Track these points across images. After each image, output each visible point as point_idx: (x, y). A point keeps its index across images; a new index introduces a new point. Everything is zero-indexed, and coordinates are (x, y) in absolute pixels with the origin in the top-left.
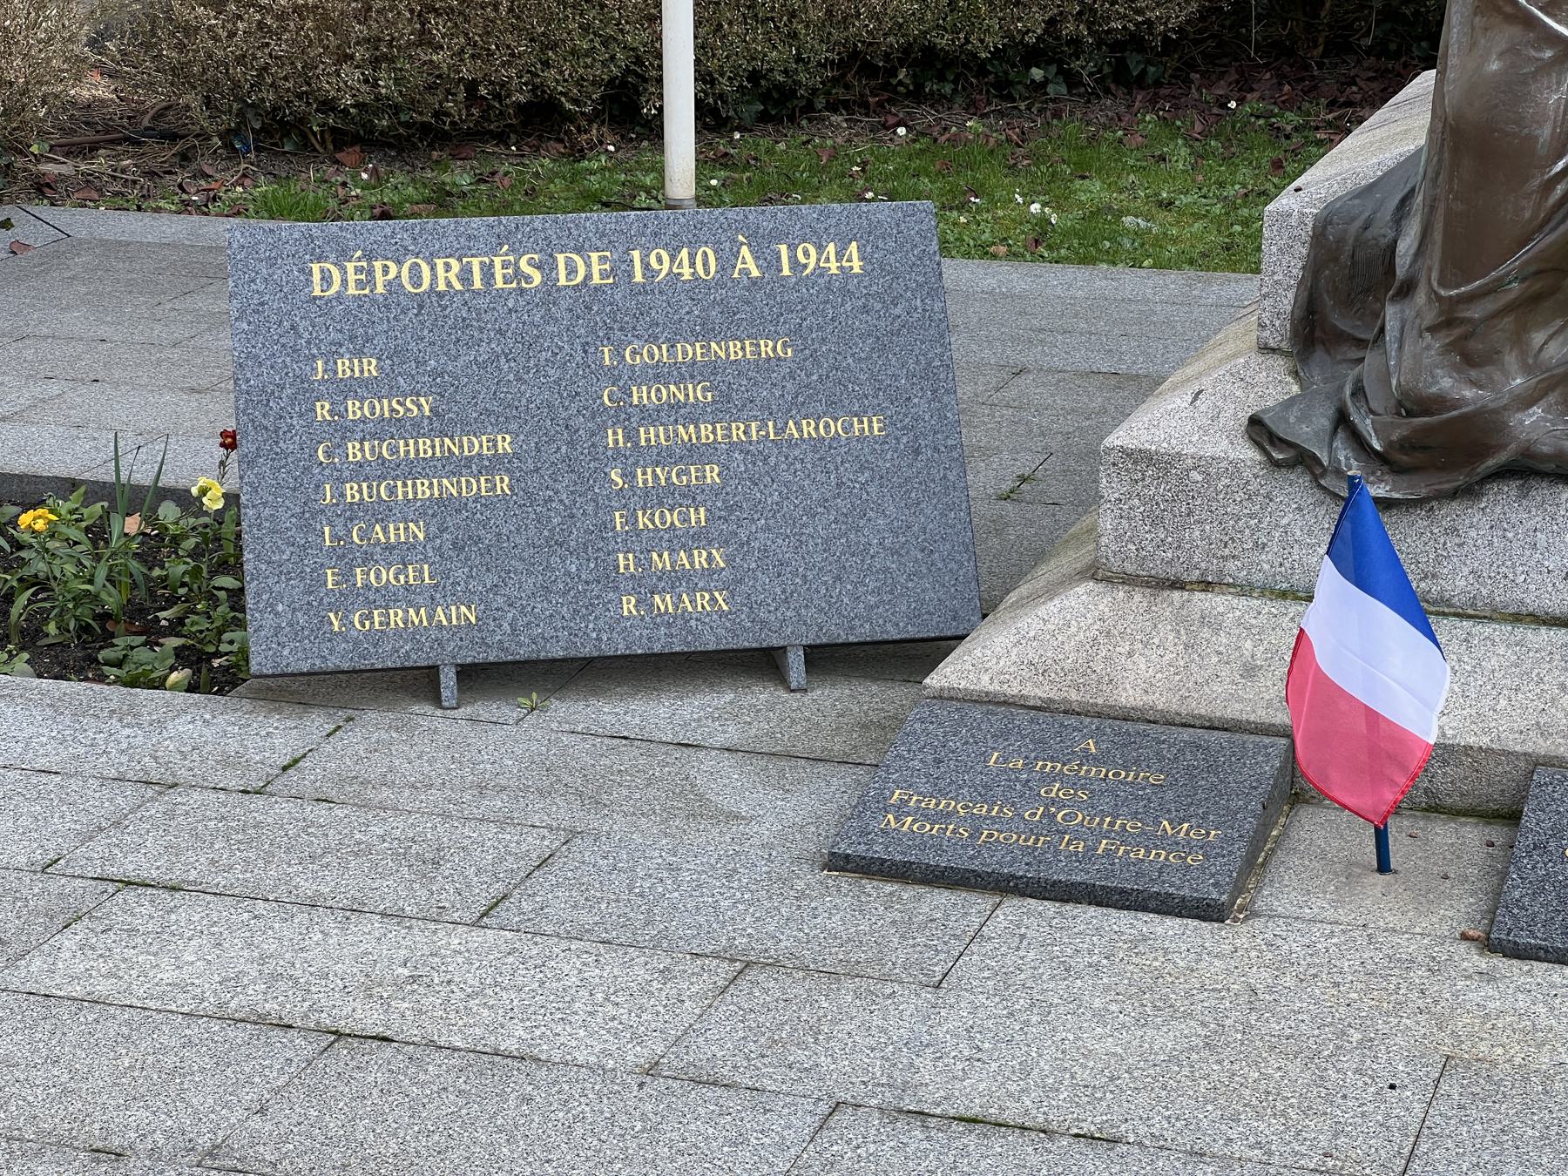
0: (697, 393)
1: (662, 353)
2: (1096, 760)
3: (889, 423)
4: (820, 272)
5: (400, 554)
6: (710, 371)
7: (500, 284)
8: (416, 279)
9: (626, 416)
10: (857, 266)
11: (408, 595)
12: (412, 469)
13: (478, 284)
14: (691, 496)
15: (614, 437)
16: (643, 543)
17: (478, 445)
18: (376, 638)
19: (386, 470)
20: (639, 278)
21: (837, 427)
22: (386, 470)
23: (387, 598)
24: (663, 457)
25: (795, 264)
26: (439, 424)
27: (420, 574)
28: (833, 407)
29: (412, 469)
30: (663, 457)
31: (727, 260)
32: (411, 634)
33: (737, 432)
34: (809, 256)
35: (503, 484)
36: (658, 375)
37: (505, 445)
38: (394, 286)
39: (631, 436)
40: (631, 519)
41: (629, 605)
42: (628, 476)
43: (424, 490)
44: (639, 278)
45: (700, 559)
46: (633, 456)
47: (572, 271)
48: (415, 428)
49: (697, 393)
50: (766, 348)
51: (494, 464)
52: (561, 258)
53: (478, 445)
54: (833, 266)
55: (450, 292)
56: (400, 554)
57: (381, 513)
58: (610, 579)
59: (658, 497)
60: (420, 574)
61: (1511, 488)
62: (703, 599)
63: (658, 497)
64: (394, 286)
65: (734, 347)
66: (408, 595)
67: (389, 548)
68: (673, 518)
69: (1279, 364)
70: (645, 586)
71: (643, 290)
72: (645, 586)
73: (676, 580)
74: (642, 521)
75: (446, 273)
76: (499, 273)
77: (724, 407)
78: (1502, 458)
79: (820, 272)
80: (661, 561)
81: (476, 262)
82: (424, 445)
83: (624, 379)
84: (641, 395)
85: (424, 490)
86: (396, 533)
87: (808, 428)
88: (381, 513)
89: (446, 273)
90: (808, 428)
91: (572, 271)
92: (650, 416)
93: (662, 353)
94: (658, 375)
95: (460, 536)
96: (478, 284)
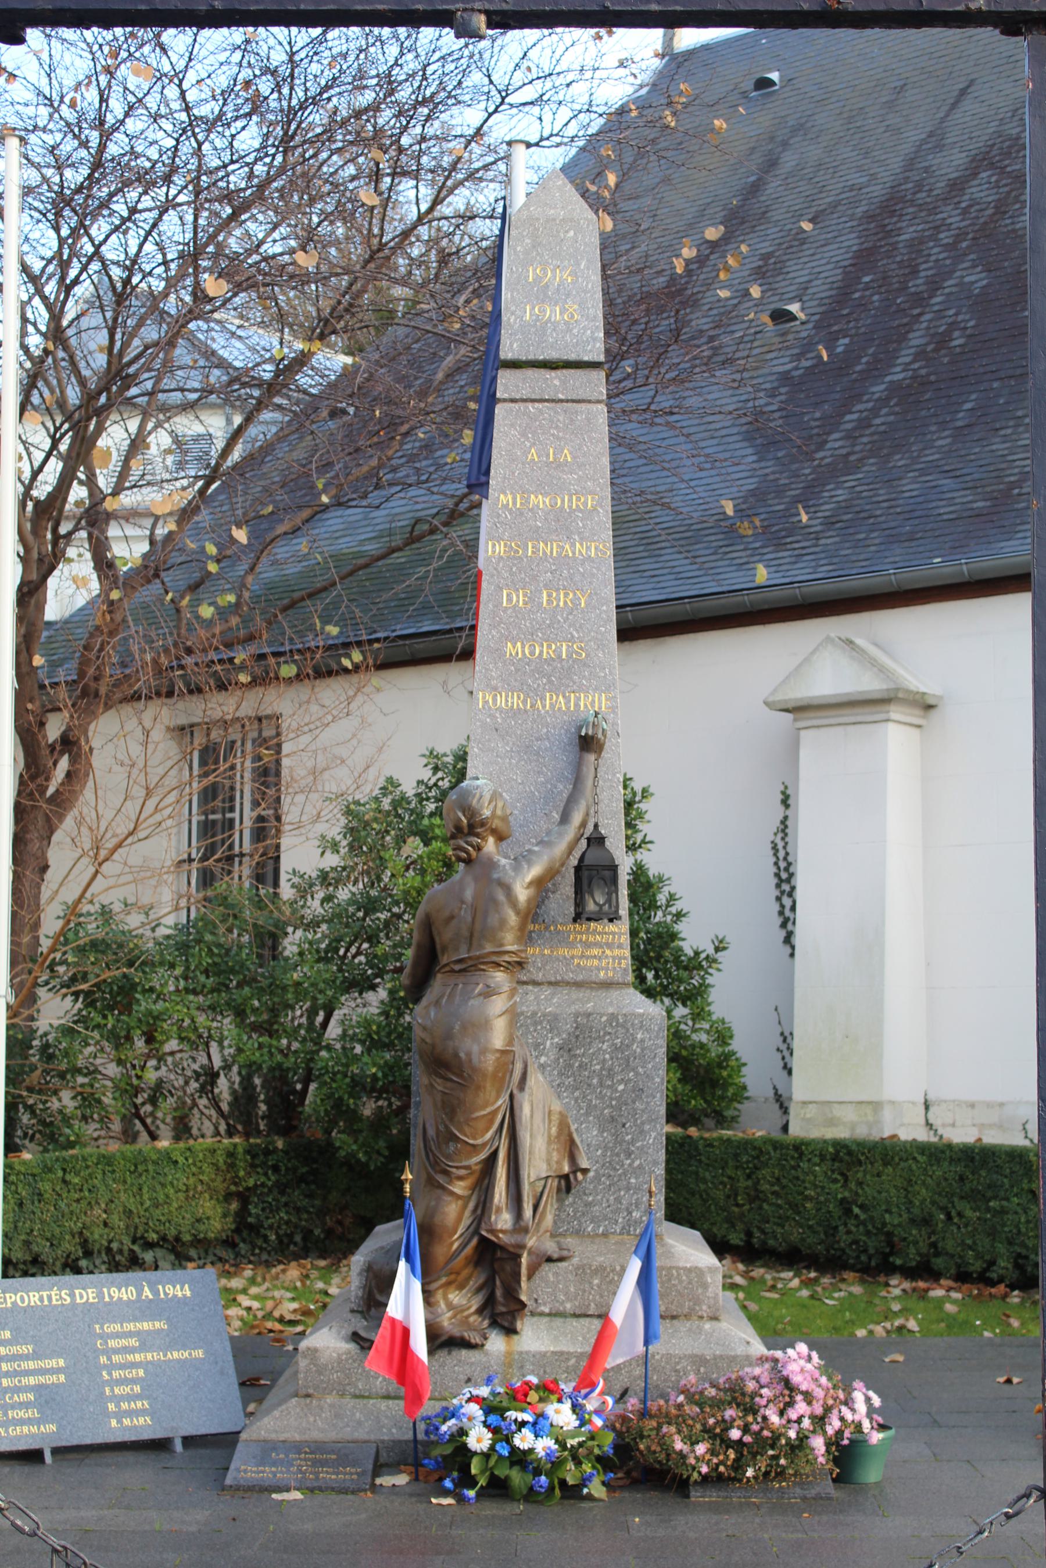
0: (133, 1342)
1: (118, 1327)
2: (311, 1453)
3: (206, 1353)
4: (175, 1296)
5: (25, 1405)
6: (137, 1334)
7: (54, 1302)
8: (22, 1299)
9: (109, 1352)
10: (188, 1293)
11: (29, 1422)
12: (28, 1373)
13: (46, 1302)
14: (134, 1381)
15: (103, 1360)
16: (118, 1399)
17: (52, 1363)
18: (19, 1438)
19: (16, 1374)
20: (107, 1299)
21: (186, 1354)
22: (16, 1374)
23: (22, 1422)
24: (122, 1366)
25: (166, 1294)
26: (36, 1356)
27: (33, 1413)
28: (184, 1347)
29: (28, 1373)
30: (122, 1366)
31: (140, 1292)
32: (33, 1436)
33: (149, 1357)
34: (170, 1290)
35: (62, 1378)
36: (117, 1335)
37: (62, 1363)
38: (14, 1303)
39: (109, 1359)
40: (112, 1390)
41: (114, 1423)
42: (110, 1374)
43: (32, 1381)
44: (107, 1299)
45: (139, 1404)
46: (111, 1367)
47: (81, 1297)
48: (26, 1357)
49: (133, 1342)
50: (157, 1325)
51: (57, 1371)
52: (77, 1292)
53: (52, 1363)
54: (180, 1294)
55: (37, 1306)
56: (25, 1405)
57: (17, 1390)
58: (108, 1415)
59: (121, 1382)
60: (33, 1413)
61: (445, 1352)
62: (141, 1420)
63: (121, 1382)
64: (14, 1303)
65: (145, 1324)
66: (29, 1422)
67: (21, 1403)
68: (128, 1389)
69: (359, 1316)
70: (120, 1415)
71: (109, 1304)
72: (120, 1415)
73: (130, 1413)
74: (116, 1391)
75: (34, 1298)
76: (54, 1298)
77: (143, 1347)
78: (444, 1338)
79: (175, 1296)
80: (124, 1406)
81: (45, 1294)
82: (31, 1363)
83: (105, 1337)
84: (112, 1343)
85: (32, 1381)
86: (23, 1397)
87: (176, 1355)
88: (17, 1390)
89: (34, 1298)
90: (176, 1355)
91: (81, 1297)
92: (116, 1351)
93: (118, 1327)
94: (117, 1335)
95: (47, 1399)
96: (46, 1302)
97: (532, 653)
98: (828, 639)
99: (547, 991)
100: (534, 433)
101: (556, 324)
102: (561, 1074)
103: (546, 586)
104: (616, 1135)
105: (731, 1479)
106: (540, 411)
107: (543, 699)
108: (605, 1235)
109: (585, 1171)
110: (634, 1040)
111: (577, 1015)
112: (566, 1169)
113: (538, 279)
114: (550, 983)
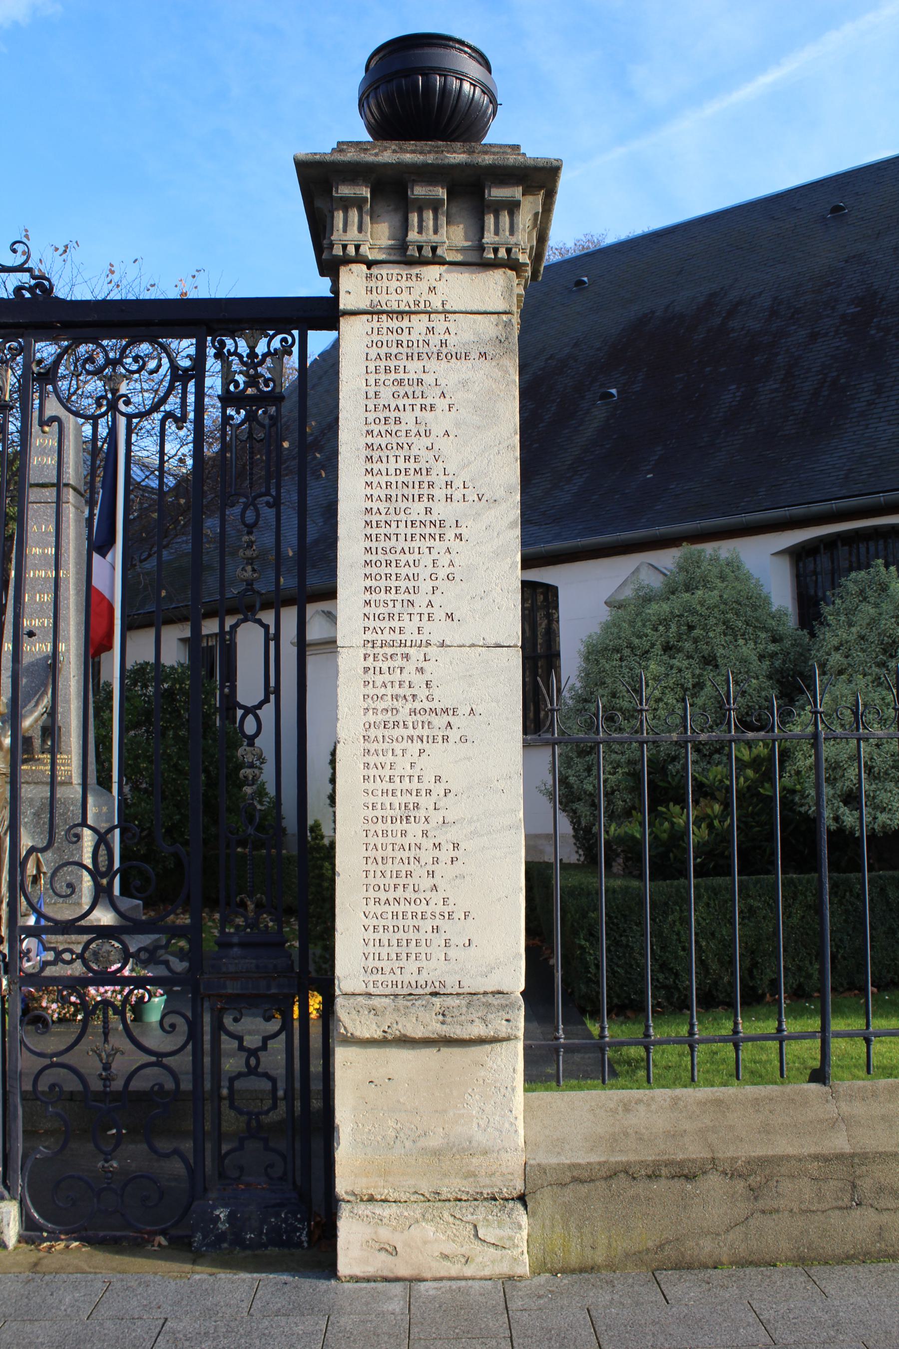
97: (31, 624)
98: (317, 612)
99: (32, 786)
100: (36, 518)
101: (48, 466)
102: (34, 827)
103: (39, 592)
104: (60, 856)
105: (70, 1020)
106: (39, 508)
107: (35, 646)
108: (55, 904)
109: (45, 873)
110: (69, 810)
111: (42, 798)
112: (35, 872)
113: (41, 444)
114: (35, 783)
